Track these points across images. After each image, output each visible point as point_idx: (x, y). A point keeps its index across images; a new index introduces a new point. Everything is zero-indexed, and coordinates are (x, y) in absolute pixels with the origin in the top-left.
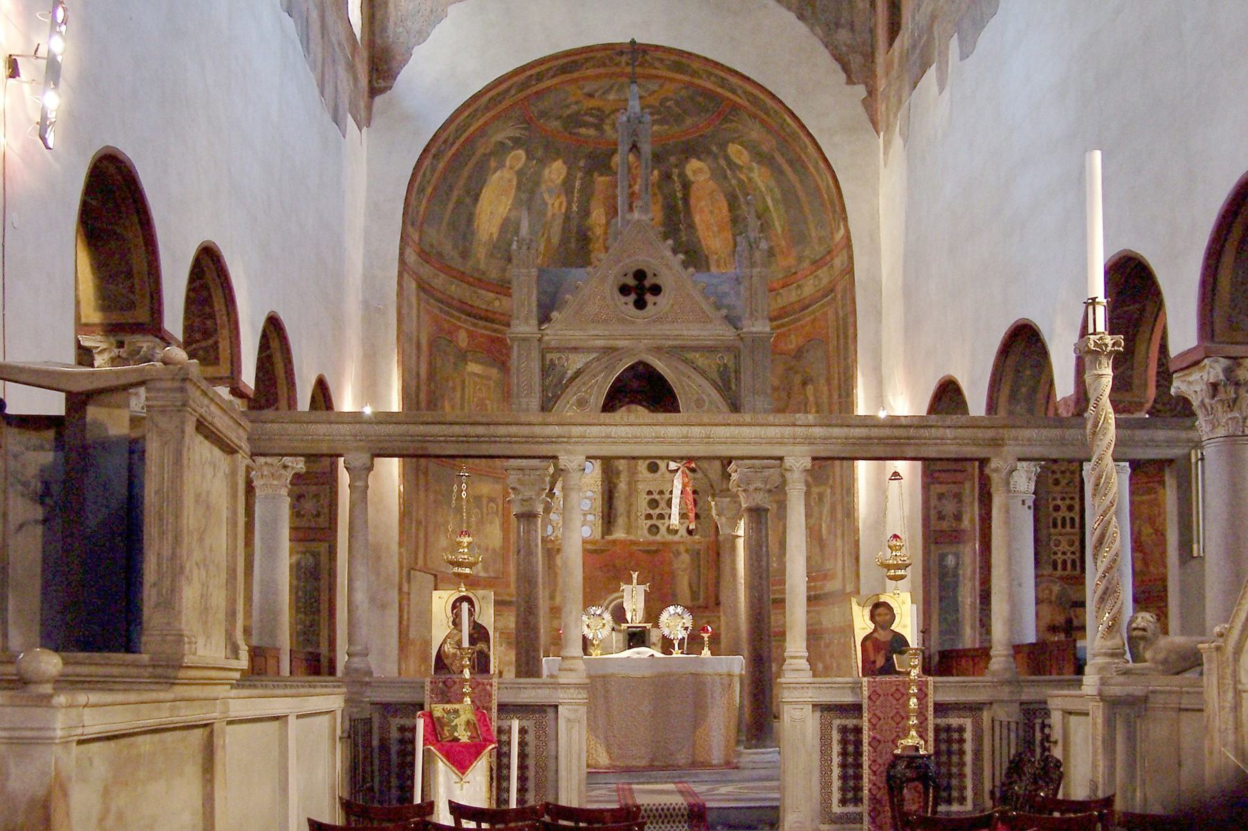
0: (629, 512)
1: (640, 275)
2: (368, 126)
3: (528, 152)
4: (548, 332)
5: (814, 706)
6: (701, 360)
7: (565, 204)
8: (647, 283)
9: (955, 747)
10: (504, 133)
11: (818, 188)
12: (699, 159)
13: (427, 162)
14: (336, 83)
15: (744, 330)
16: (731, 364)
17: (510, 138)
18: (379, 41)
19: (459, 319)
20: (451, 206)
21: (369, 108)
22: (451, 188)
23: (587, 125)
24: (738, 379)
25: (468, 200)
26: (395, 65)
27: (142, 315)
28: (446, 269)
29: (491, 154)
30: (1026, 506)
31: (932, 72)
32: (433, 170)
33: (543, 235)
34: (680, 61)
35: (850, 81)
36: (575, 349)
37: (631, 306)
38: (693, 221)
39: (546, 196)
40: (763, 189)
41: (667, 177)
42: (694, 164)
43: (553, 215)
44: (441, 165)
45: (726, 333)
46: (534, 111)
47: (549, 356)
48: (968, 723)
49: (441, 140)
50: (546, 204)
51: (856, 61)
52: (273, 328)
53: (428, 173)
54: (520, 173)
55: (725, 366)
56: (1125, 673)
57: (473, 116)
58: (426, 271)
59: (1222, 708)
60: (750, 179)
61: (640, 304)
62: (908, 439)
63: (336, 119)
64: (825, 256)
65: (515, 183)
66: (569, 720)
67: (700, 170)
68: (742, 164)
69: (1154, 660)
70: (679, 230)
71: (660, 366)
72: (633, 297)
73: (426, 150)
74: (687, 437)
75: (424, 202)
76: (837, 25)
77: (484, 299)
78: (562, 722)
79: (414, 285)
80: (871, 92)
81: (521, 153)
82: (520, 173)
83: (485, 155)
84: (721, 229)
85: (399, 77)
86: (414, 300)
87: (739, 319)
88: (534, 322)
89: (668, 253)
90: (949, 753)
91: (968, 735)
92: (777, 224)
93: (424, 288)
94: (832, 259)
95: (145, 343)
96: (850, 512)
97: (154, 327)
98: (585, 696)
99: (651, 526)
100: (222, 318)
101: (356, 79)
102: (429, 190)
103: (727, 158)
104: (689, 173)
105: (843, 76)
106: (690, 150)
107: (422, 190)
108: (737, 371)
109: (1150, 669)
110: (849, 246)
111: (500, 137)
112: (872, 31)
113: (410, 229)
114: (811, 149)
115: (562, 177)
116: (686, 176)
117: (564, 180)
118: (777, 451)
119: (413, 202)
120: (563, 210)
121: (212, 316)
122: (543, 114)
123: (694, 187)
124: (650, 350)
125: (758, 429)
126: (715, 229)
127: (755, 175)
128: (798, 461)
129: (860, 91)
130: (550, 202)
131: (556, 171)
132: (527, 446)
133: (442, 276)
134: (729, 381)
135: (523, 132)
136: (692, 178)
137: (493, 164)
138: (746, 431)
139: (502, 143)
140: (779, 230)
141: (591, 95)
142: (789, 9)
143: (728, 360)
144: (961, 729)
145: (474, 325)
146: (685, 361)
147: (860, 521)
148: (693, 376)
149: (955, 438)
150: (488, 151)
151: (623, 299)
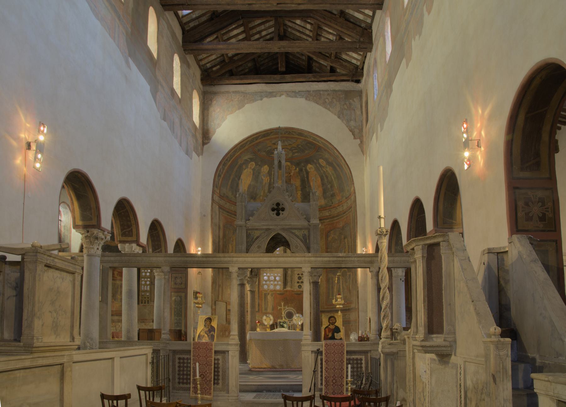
0: (291, 281)
1: (278, 204)
3: (255, 163)
4: (248, 223)
5: (312, 351)
6: (297, 232)
7: (269, 180)
8: (280, 207)
9: (359, 365)
11: (346, 174)
12: (311, 164)
13: (221, 167)
14: (187, 143)
15: (311, 222)
16: (307, 234)
17: (249, 158)
20: (230, 181)
24: (309, 239)
25: (236, 179)
30: (402, 281)
32: (223, 169)
33: (262, 190)
34: (300, 133)
36: (257, 229)
37: (275, 215)
38: (310, 185)
39: (263, 177)
40: (331, 174)
41: (301, 170)
42: (309, 166)
43: (266, 183)
44: (226, 168)
45: (305, 223)
48: (363, 357)
49: (225, 159)
50: (262, 179)
53: (221, 170)
54: (254, 170)
55: (305, 234)
56: (390, 344)
57: (235, 152)
59: (409, 358)
60: (327, 171)
61: (278, 214)
62: (343, 261)
64: (349, 196)
65: (252, 173)
66: (232, 356)
67: (311, 168)
68: (324, 166)
69: (400, 340)
70: (306, 187)
71: (284, 234)
72: (275, 212)
74: (270, 261)
75: (221, 180)
78: (230, 357)
79: (217, 207)
81: (253, 163)
83: (241, 164)
88: (244, 220)
89: (287, 197)
90: (357, 368)
91: (363, 362)
92: (335, 185)
93: (220, 207)
94: (351, 197)
96: (356, 281)
98: (237, 348)
99: (299, 285)
100: (133, 222)
102: (222, 176)
103: (319, 164)
104: (308, 169)
106: (308, 161)
107: (219, 176)
108: (309, 236)
109: (398, 343)
110: (355, 193)
111: (246, 158)
113: (215, 189)
114: (343, 161)
115: (267, 171)
116: (307, 169)
117: (268, 172)
118: (299, 266)
119: (216, 180)
120: (269, 181)
121: (130, 221)
123: (310, 174)
125: (293, 258)
126: (317, 187)
127: (328, 169)
128: (306, 269)
130: (264, 179)
131: (265, 169)
132: (219, 264)
134: (306, 239)
135: (254, 156)
136: (309, 171)
137: (244, 167)
138: (289, 259)
139: (246, 160)
140: (336, 188)
143: (306, 232)
144: (361, 360)
146: (292, 233)
147: (359, 284)
148: (294, 238)
149: (358, 261)
150: (242, 163)
151: (272, 212)
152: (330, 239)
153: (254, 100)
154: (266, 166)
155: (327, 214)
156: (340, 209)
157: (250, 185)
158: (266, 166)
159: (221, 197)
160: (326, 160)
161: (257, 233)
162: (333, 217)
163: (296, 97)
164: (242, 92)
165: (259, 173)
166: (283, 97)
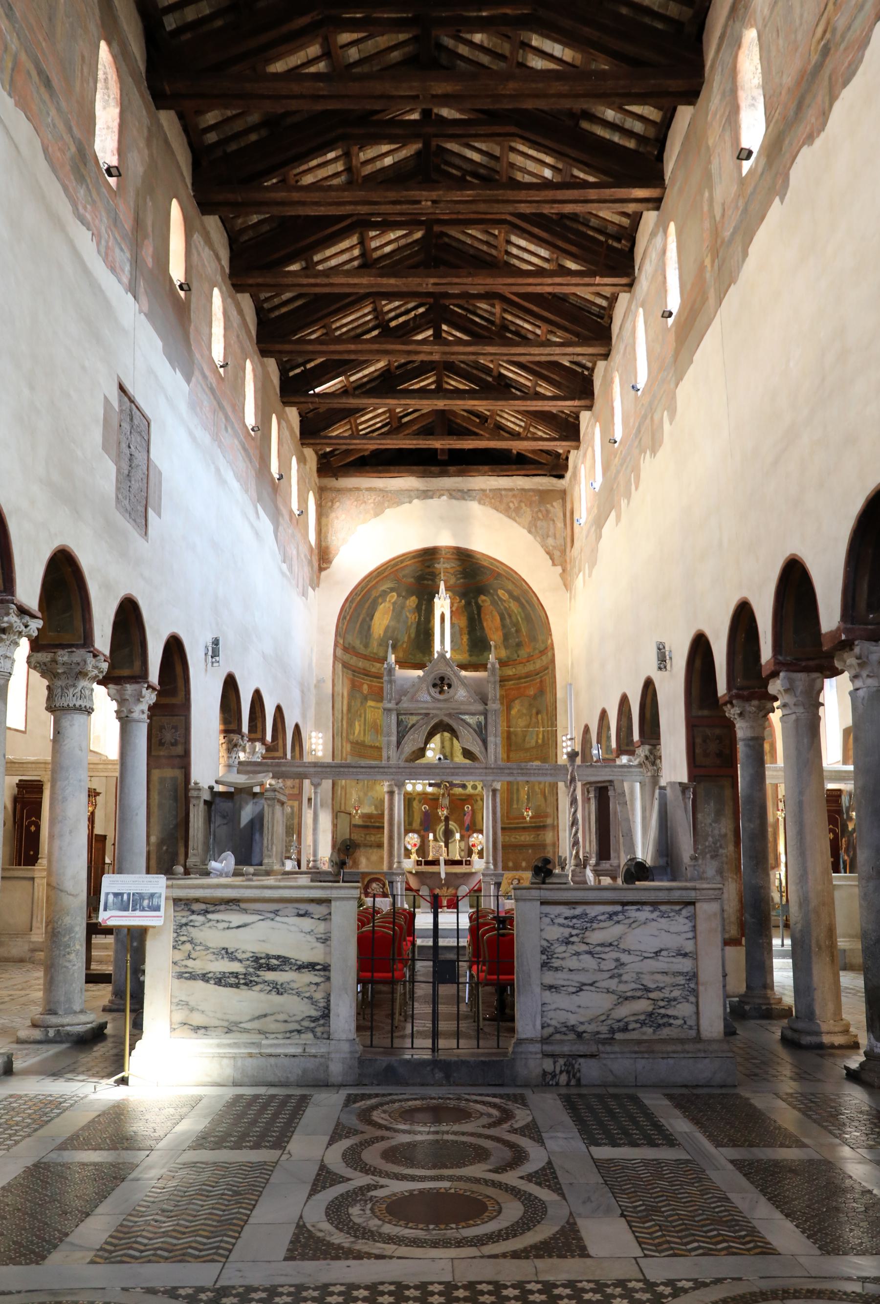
2: (318, 585)
10: (385, 587)
13: (347, 605)
18: (323, 544)
19: (363, 679)
21: (319, 578)
22: (359, 615)
23: (428, 580)
26: (331, 556)
27: (233, 727)
28: (357, 654)
29: (380, 596)
31: (581, 575)
35: (554, 564)
41: (468, 604)
42: (483, 597)
44: (354, 605)
46: (401, 575)
47: (400, 717)
50: (407, 617)
51: (557, 554)
52: (279, 709)
57: (369, 581)
58: (347, 657)
61: (441, 692)
63: (303, 595)
73: (347, 600)
76: (548, 536)
77: (375, 668)
80: (564, 570)
81: (395, 594)
82: (394, 604)
84: (497, 629)
85: (334, 562)
86: (340, 674)
87: (487, 699)
93: (345, 665)
95: (236, 737)
97: (239, 731)
101: (312, 567)
102: (348, 618)
103: (498, 596)
104: (480, 602)
105: (550, 562)
111: (383, 588)
112: (564, 539)
113: (339, 638)
114: (535, 598)
119: (340, 625)
122: (404, 576)
124: (446, 715)
129: (559, 569)
130: (409, 616)
131: (412, 601)
133: (355, 658)
137: (380, 600)
139: (384, 591)
141: (429, 567)
142: (524, 528)
145: (371, 681)
152: (513, 712)
153: (400, 503)
154: (414, 598)
155: (510, 672)
156: (530, 667)
157: (387, 628)
158: (414, 598)
159: (346, 649)
160: (510, 593)
161: (413, 719)
162: (520, 678)
163: (464, 499)
164: (381, 490)
165: (403, 607)
166: (444, 498)
